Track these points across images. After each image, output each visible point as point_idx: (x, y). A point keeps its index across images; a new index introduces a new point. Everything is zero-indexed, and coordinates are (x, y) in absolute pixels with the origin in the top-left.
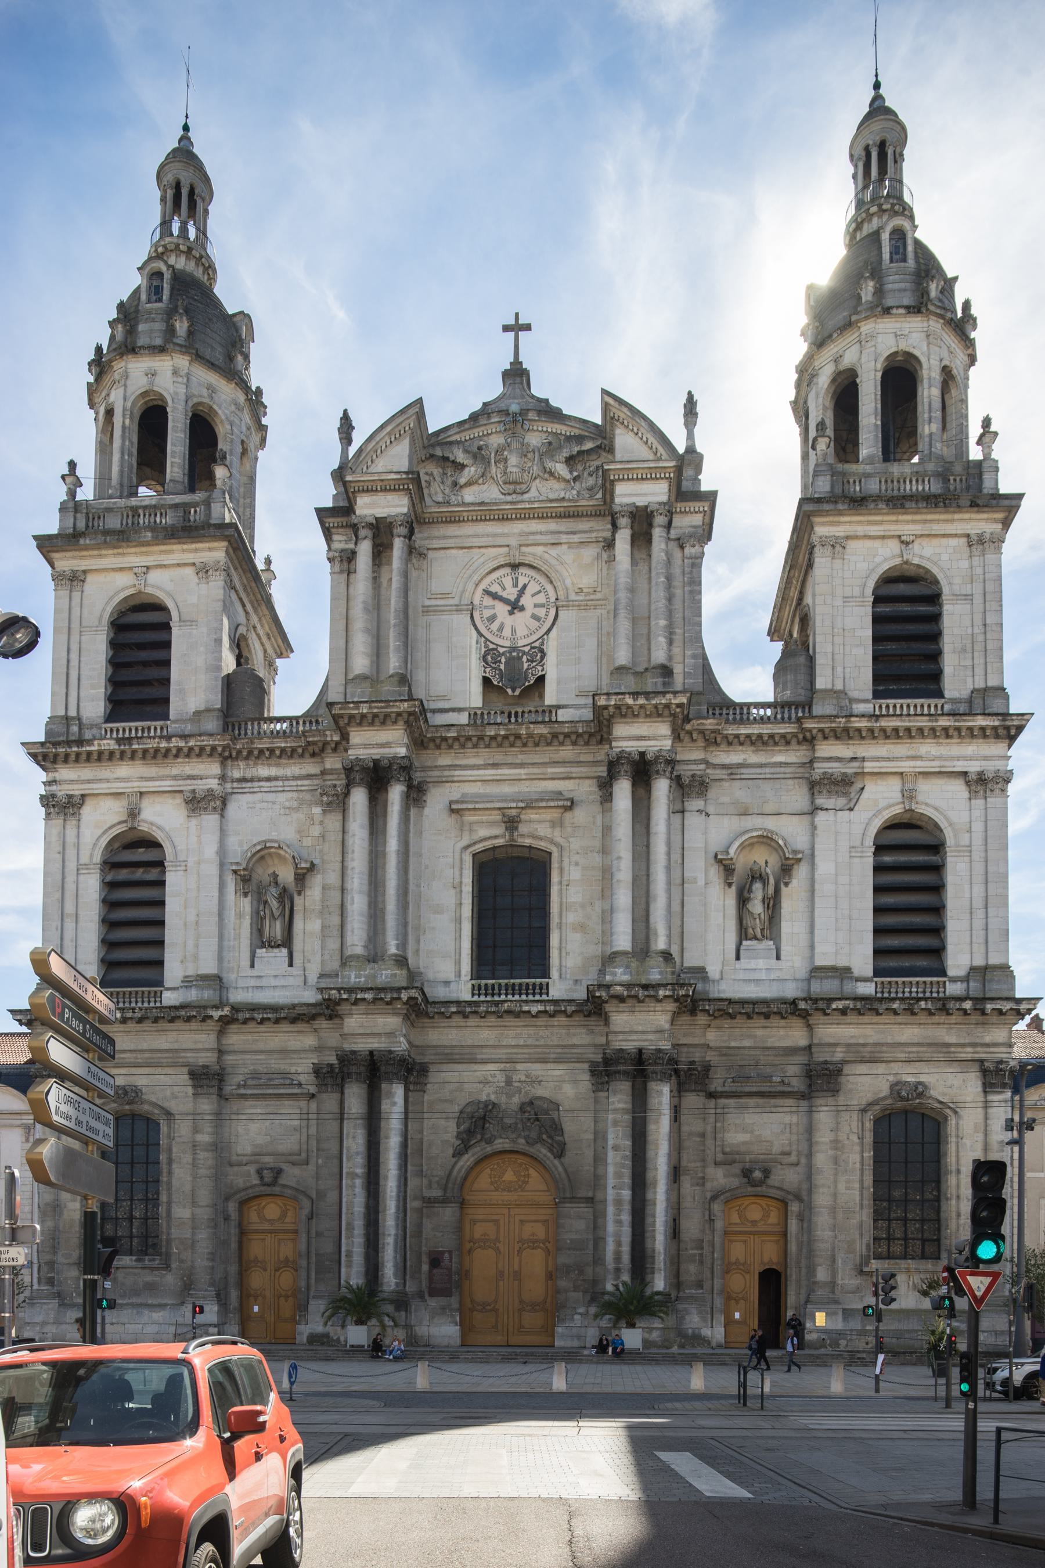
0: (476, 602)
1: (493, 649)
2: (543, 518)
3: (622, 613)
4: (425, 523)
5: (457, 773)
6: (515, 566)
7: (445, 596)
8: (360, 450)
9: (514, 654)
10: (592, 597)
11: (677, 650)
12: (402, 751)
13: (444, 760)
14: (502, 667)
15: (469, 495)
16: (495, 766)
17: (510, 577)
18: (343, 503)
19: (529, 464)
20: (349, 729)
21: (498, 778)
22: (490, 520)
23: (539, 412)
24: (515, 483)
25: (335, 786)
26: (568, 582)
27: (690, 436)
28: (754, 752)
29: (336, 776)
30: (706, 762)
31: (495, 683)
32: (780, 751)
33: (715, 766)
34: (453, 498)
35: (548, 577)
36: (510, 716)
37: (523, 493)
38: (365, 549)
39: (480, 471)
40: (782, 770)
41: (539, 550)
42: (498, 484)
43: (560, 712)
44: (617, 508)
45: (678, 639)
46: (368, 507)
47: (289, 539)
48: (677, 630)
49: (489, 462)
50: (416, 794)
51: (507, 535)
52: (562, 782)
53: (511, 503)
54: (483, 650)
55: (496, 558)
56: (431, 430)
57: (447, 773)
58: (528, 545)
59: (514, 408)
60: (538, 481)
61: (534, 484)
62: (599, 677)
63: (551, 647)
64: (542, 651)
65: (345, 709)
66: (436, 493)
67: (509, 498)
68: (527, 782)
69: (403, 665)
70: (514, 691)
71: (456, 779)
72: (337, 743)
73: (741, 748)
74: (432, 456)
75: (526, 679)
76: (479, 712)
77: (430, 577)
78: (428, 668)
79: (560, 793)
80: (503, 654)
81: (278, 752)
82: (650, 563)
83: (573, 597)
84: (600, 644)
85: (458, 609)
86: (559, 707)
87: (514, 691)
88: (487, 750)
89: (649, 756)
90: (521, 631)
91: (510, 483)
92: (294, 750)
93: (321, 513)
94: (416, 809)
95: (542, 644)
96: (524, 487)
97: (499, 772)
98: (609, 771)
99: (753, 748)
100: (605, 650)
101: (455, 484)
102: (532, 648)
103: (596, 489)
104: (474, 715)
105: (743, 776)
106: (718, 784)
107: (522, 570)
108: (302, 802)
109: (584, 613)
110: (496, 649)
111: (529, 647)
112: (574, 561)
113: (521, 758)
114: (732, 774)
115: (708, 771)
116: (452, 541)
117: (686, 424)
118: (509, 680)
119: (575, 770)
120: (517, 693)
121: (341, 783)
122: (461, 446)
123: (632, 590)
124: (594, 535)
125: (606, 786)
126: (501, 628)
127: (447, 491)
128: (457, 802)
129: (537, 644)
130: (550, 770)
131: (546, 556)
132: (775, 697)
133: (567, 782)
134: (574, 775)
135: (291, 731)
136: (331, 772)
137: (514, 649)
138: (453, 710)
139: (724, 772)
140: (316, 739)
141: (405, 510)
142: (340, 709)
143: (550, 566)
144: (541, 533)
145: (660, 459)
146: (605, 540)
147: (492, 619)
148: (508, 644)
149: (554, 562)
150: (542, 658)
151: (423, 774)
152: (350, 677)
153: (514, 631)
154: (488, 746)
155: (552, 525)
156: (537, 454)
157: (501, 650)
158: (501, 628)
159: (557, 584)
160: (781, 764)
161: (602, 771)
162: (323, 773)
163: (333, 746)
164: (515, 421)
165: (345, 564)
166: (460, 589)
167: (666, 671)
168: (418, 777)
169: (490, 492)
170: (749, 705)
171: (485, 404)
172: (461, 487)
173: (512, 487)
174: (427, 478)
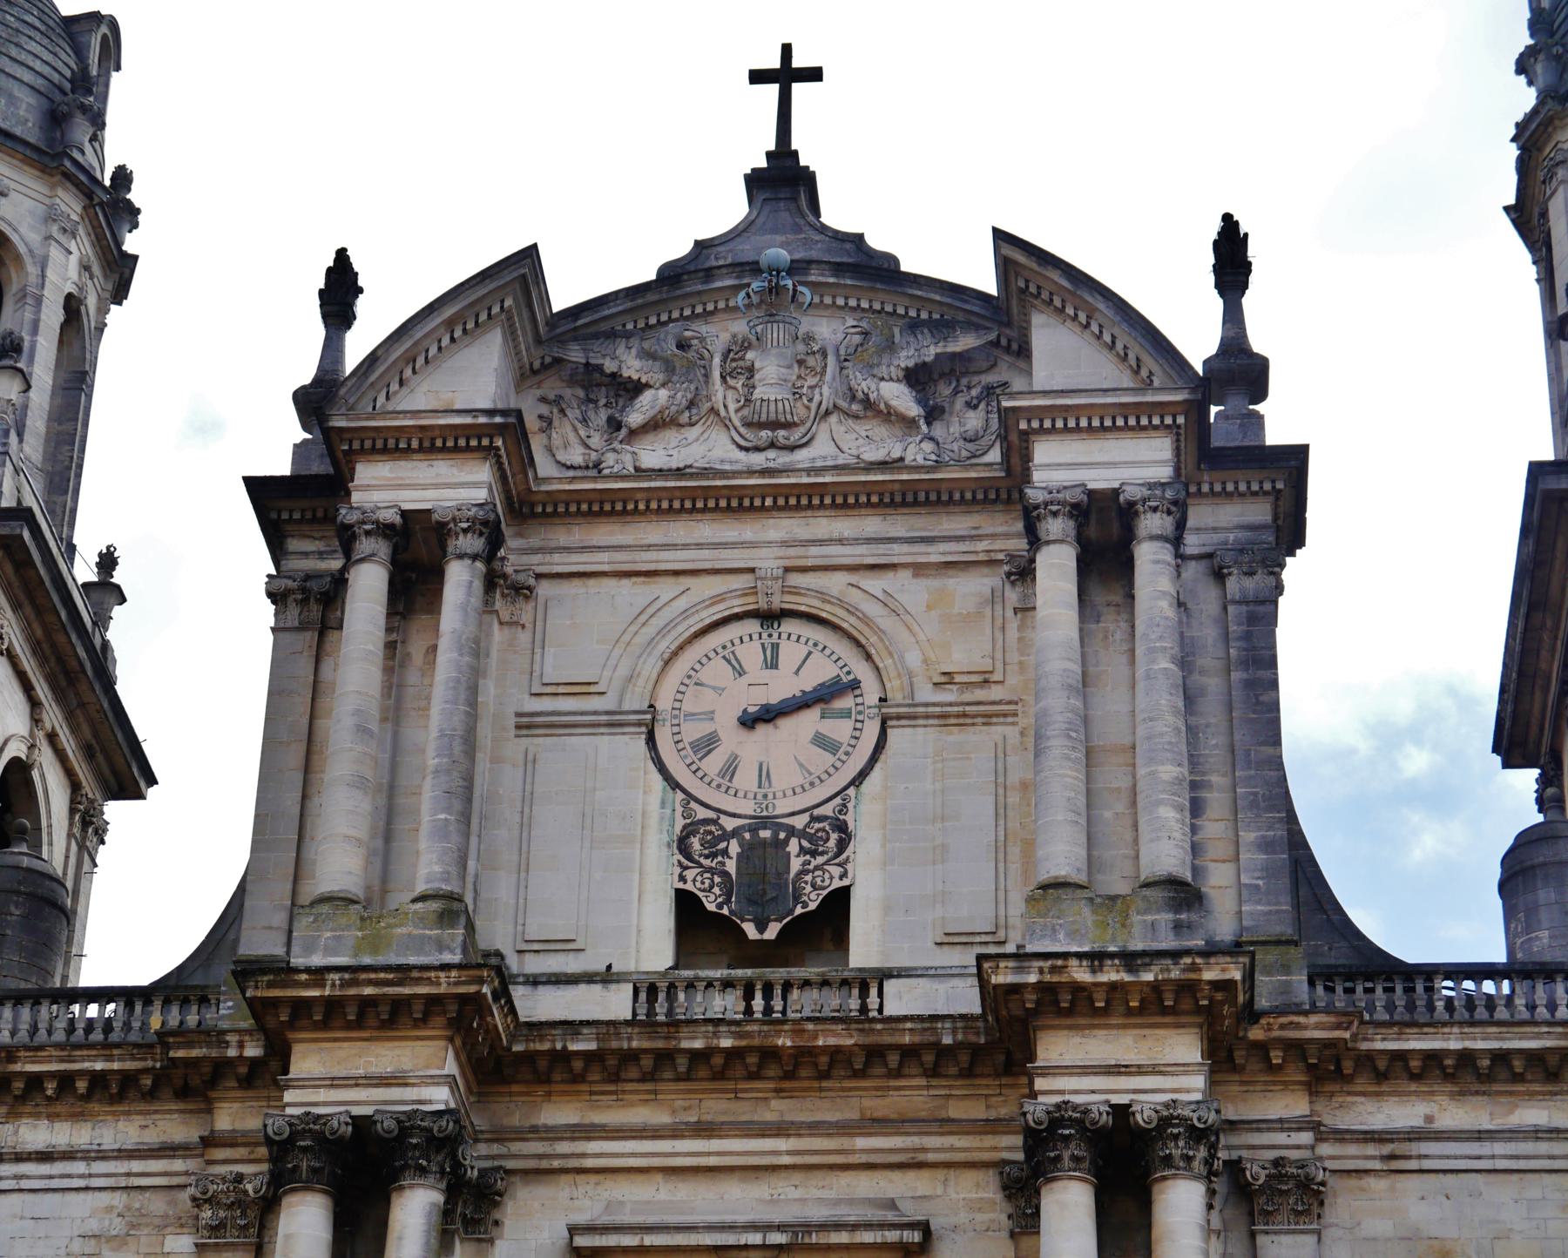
0: (664, 704)
1: (706, 821)
2: (845, 505)
3: (1057, 746)
4: (534, 515)
5: (594, 1146)
6: (770, 617)
7: (582, 689)
8: (372, 359)
9: (765, 834)
10: (980, 694)
11: (1214, 828)
12: (439, 1097)
13: (560, 1113)
14: (731, 866)
15: (655, 454)
16: (704, 1130)
17: (756, 644)
18: (320, 467)
19: (811, 381)
20: (291, 1035)
21: (713, 1161)
22: (705, 510)
23: (838, 269)
24: (774, 425)
25: (239, 1178)
26: (913, 659)
27: (1233, 316)
28: (1452, 1095)
29: (241, 1152)
30: (1315, 1127)
31: (711, 907)
32: (1532, 1094)
33: (1341, 1136)
34: (610, 459)
35: (858, 644)
36: (749, 996)
37: (792, 448)
38: (369, 585)
39: (682, 398)
40: (1543, 1147)
41: (835, 583)
42: (726, 424)
43: (890, 986)
44: (1035, 495)
45: (1217, 802)
46: (382, 488)
47: (196, 643)
48: (1215, 779)
49: (707, 376)
50: (472, 1206)
51: (753, 545)
52: (896, 1175)
53: (765, 472)
54: (680, 823)
55: (718, 599)
56: (559, 302)
57: (564, 1147)
58: (804, 570)
59: (778, 254)
60: (833, 419)
61: (824, 426)
62: (1000, 895)
63: (866, 818)
64: (842, 827)
65: (284, 985)
66: (566, 445)
67: (758, 460)
68: (797, 1177)
69: (454, 870)
70: (761, 928)
71: (589, 1163)
72: (253, 1062)
73: (1413, 1087)
74: (558, 361)
75: (797, 898)
76: (663, 985)
77: (539, 643)
78: (523, 867)
79: (892, 1205)
80: (736, 833)
81: (82, 1085)
82: (1132, 614)
83: (926, 694)
84: (1001, 811)
85: (614, 723)
86: (883, 975)
87: (761, 928)
88: (682, 1086)
89: (1144, 1116)
90: (785, 777)
91: (761, 426)
92: (128, 1081)
93: (259, 489)
94: (471, 1248)
95: (843, 808)
96: (796, 436)
97: (715, 1144)
98: (1029, 1150)
99: (1449, 1088)
100: (1013, 837)
101: (615, 425)
102: (814, 819)
103: (985, 441)
104: (647, 989)
105: (1427, 1164)
106: (1353, 1182)
107: (789, 626)
108: (135, 1222)
109: (955, 736)
110: (715, 822)
111: (805, 818)
112: (929, 608)
113: (777, 1109)
114: (1392, 1157)
115: (1325, 1149)
116: (604, 556)
117: (1221, 286)
118: (751, 901)
119: (936, 1144)
120: (772, 932)
121: (254, 1173)
122: (635, 342)
123: (1086, 683)
124: (982, 545)
125: (1022, 1192)
126: (730, 770)
127: (596, 441)
128: (591, 1229)
129: (827, 810)
130: (861, 1143)
131: (854, 597)
132: (1511, 951)
133: (911, 1175)
134: (931, 1157)
135: (127, 1026)
136: (230, 1140)
137: (763, 821)
138: (588, 978)
139: (1371, 1149)
140: (195, 1053)
141: (481, 495)
142: (270, 985)
143: (866, 620)
144: (841, 541)
145: (1148, 385)
146: (1012, 557)
147: (707, 744)
148: (747, 807)
149: (873, 609)
150: (842, 845)
151: (496, 1149)
152: (305, 899)
153: (764, 775)
154: (687, 1078)
155: (872, 525)
156: (831, 360)
157: (729, 824)
158: (730, 770)
159: (885, 663)
160: (1537, 1134)
161: (1010, 1146)
162: (209, 1142)
163: (243, 1070)
164: (775, 290)
165: (315, 611)
166: (623, 671)
167: (1183, 894)
168: (476, 1157)
169: (709, 448)
170: (1429, 973)
171: (701, 246)
172: (633, 433)
173: (765, 434)
174: (544, 409)
